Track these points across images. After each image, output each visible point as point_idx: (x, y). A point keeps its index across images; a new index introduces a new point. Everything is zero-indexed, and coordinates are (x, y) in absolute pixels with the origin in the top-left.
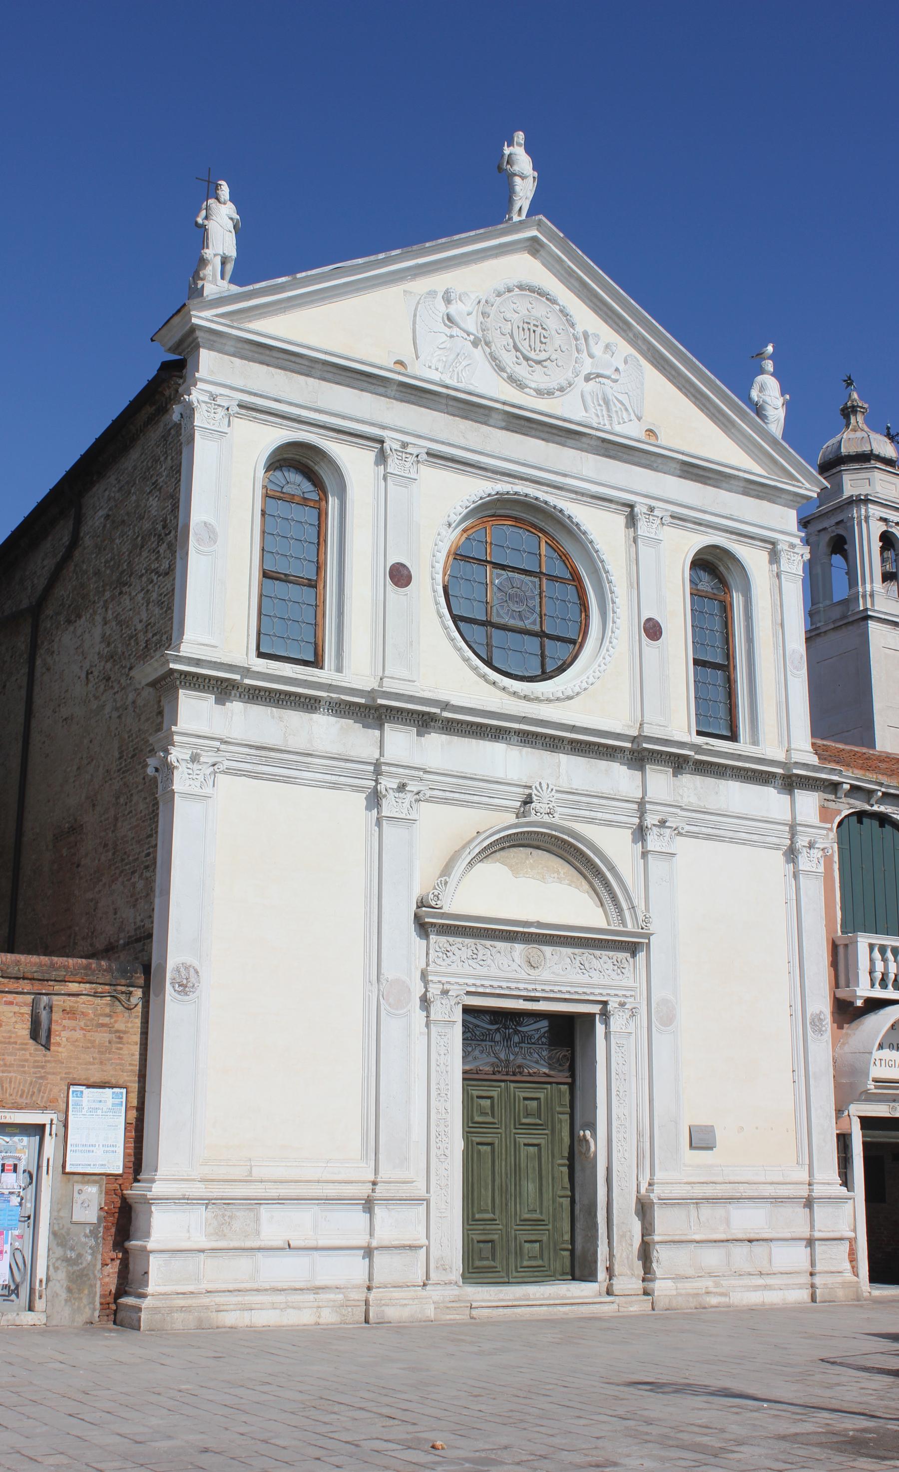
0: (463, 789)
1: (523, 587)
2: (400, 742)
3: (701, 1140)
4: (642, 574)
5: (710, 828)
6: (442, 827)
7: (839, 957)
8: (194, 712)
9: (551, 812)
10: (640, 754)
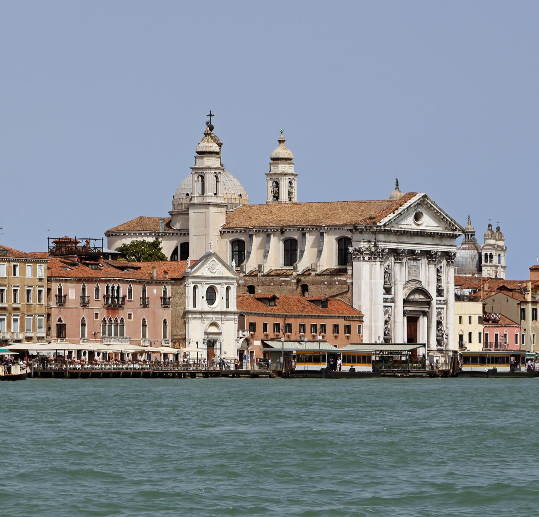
4: (221, 291)
5: (227, 320)
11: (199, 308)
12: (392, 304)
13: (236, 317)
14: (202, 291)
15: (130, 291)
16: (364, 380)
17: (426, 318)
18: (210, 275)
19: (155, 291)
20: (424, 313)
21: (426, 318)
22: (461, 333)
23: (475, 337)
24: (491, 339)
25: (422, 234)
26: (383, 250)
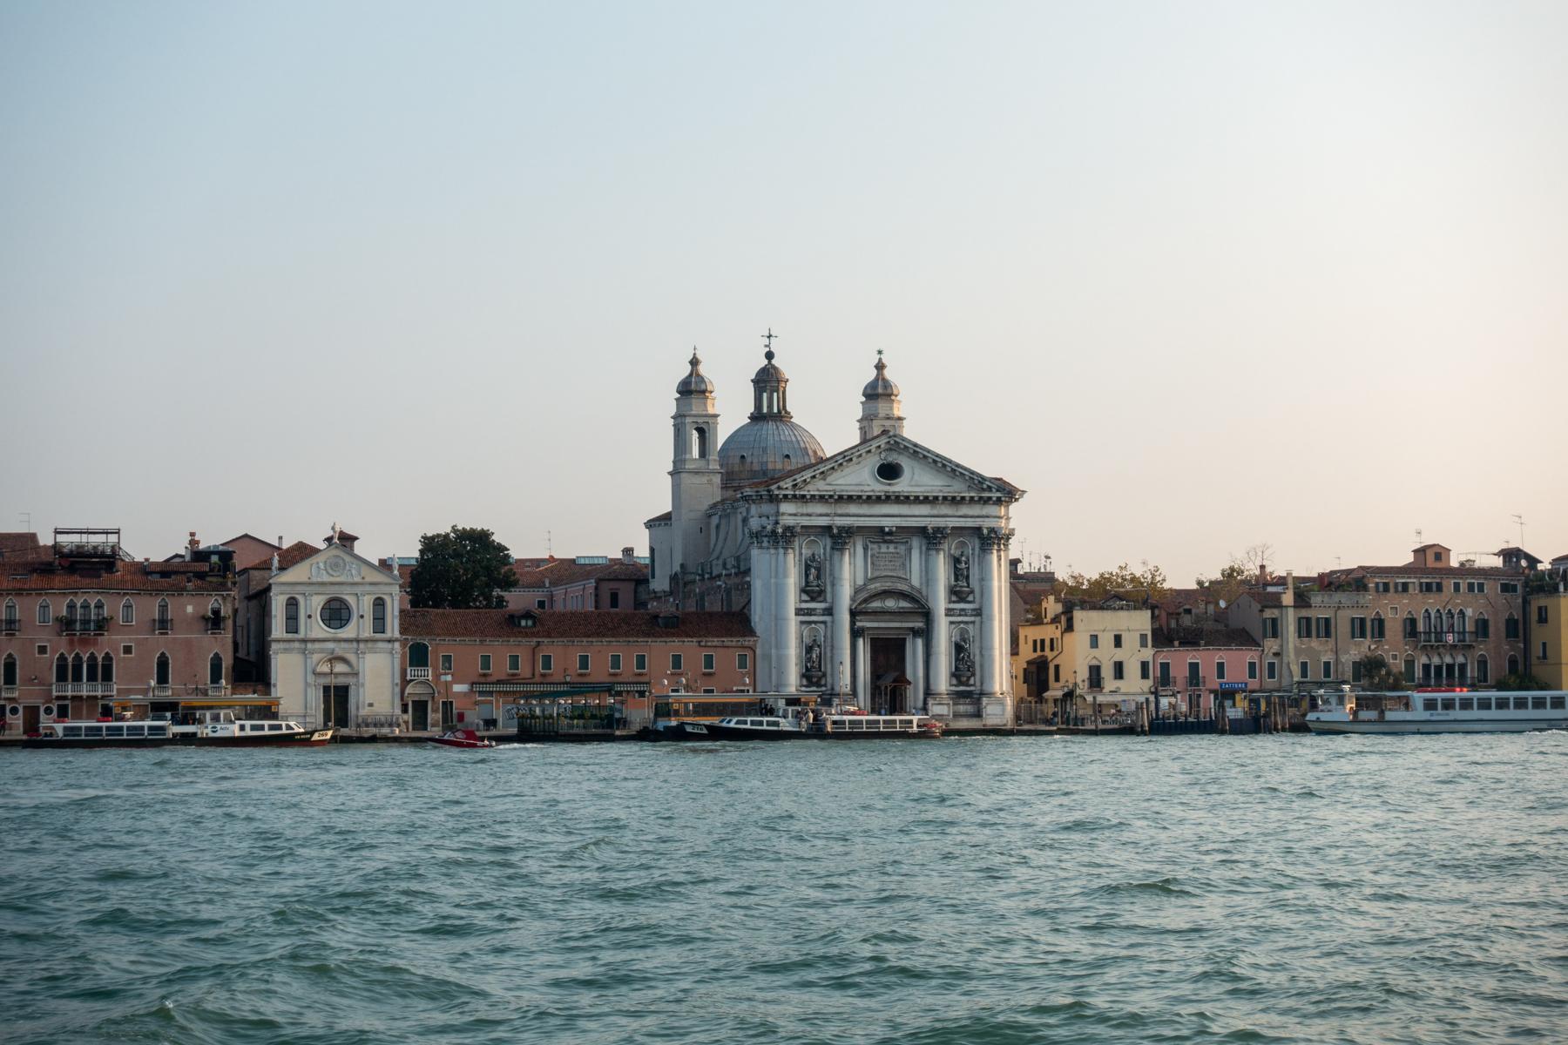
0: (322, 651)
1: (336, 613)
2: (309, 645)
3: (371, 705)
4: (362, 606)
6: (316, 657)
7: (404, 673)
8: (274, 646)
9: (339, 652)
10: (358, 641)
11: (302, 635)
12: (827, 618)
13: (397, 645)
14: (314, 604)
15: (128, 607)
16: (787, 744)
17: (920, 642)
18: (326, 578)
19: (190, 609)
20: (916, 633)
21: (920, 642)
22: (1095, 663)
23: (1132, 670)
24: (1180, 672)
25: (899, 499)
26: (788, 529)
